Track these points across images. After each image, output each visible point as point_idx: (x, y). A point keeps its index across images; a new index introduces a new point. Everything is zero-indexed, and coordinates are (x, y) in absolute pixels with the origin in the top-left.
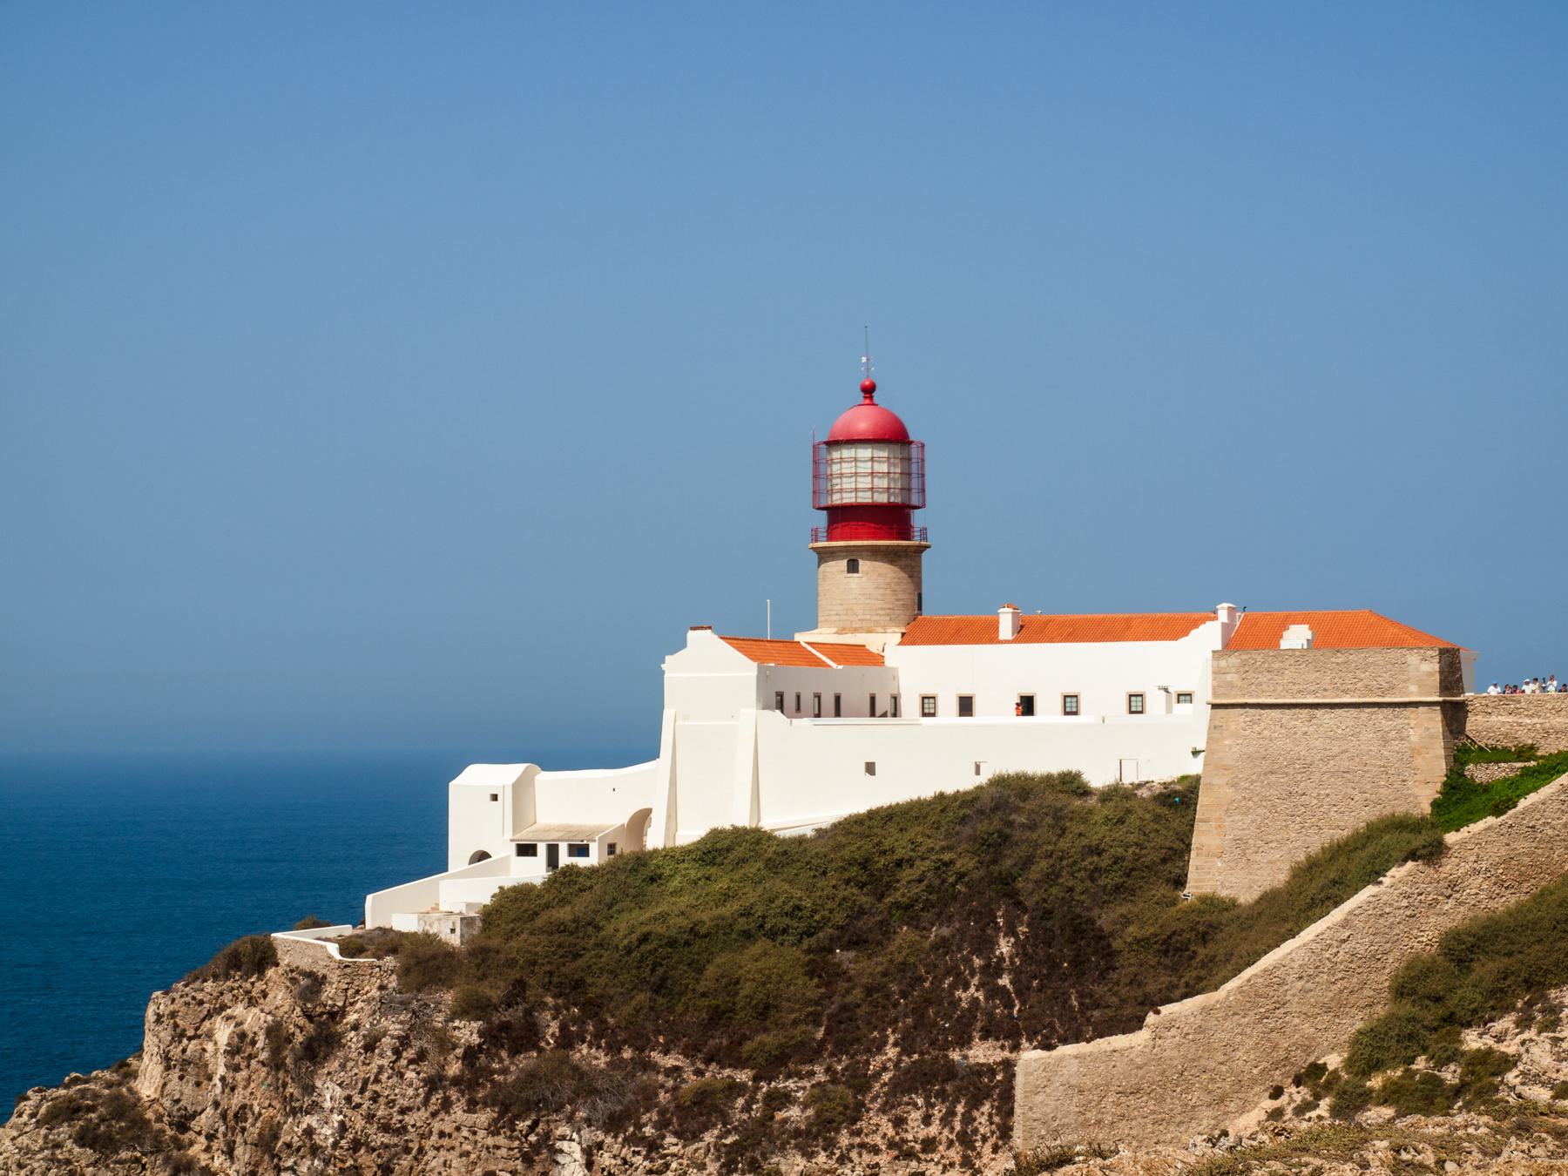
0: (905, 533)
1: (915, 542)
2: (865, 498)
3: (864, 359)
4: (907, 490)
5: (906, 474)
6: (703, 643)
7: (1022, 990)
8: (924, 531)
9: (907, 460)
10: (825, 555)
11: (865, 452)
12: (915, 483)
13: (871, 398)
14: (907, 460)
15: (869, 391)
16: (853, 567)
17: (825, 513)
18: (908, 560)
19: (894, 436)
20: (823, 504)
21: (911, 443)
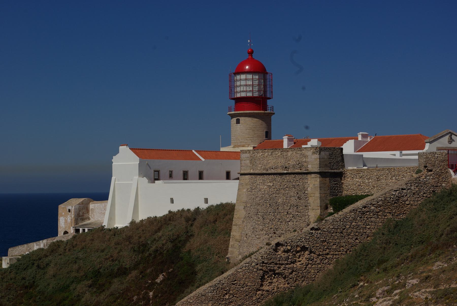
0: (265, 108)
1: (268, 111)
2: (250, 94)
3: (249, 41)
4: (265, 92)
5: (265, 86)
6: (124, 150)
7: (155, 296)
8: (272, 108)
9: (265, 80)
10: (232, 116)
11: (250, 76)
12: (268, 89)
13: (252, 56)
14: (265, 80)
15: (251, 53)
16: (238, 122)
17: (234, 101)
18: (266, 118)
19: (259, 70)
20: (233, 97)
21: (267, 73)
